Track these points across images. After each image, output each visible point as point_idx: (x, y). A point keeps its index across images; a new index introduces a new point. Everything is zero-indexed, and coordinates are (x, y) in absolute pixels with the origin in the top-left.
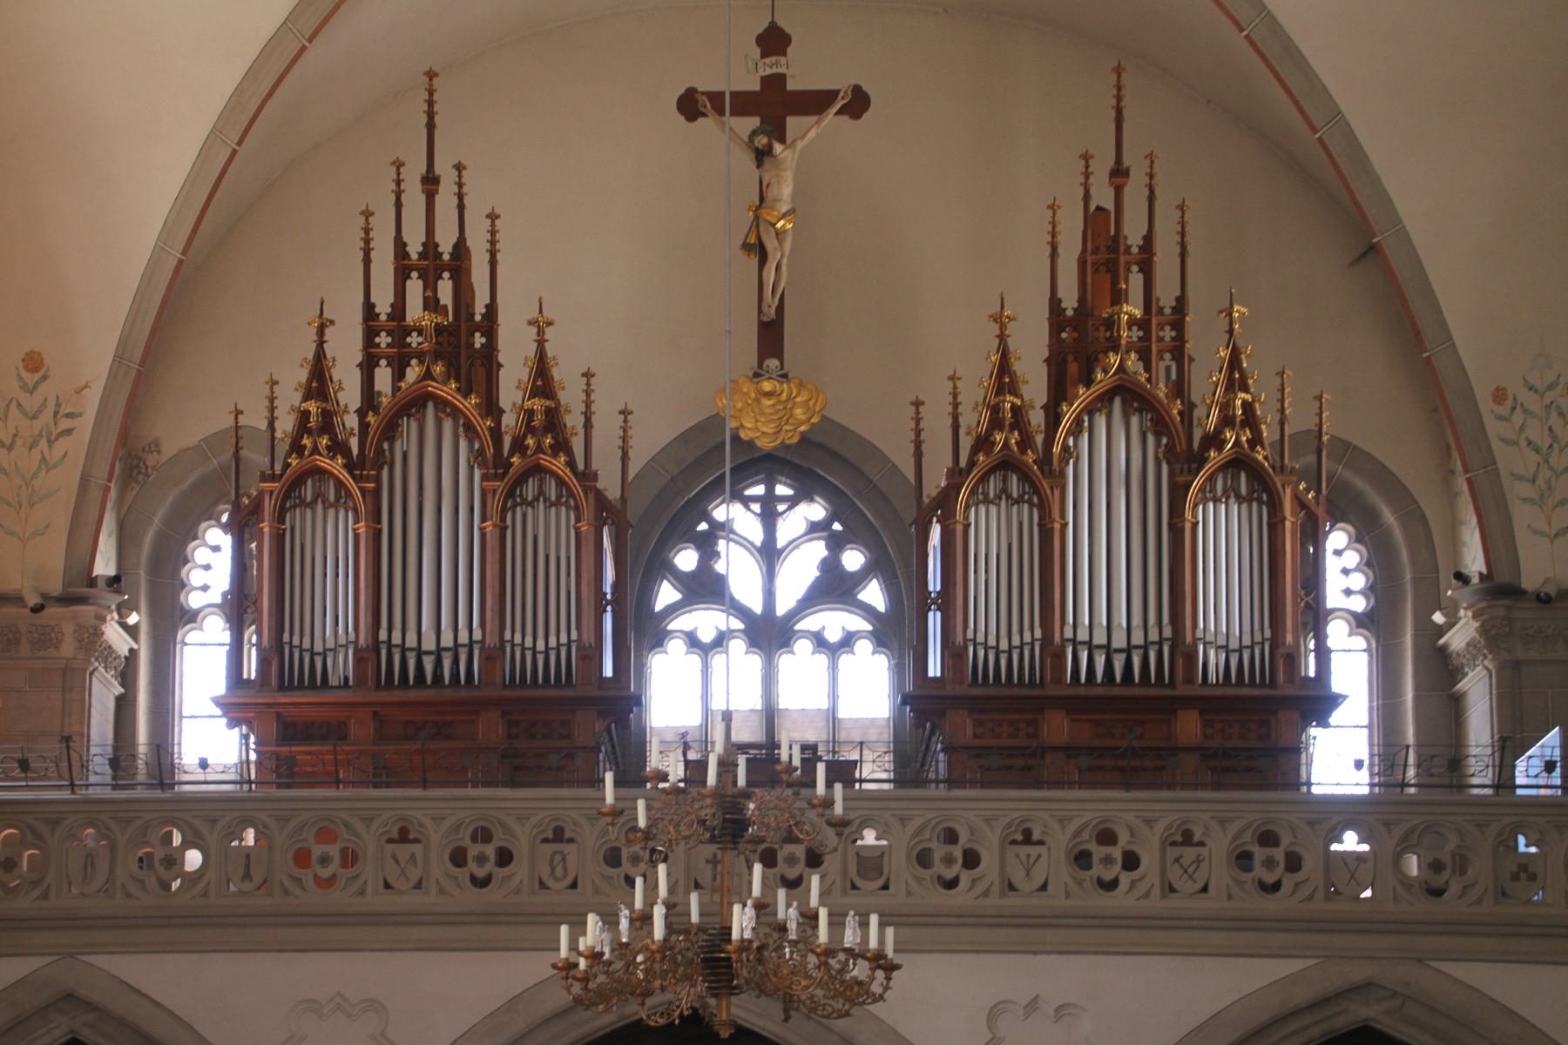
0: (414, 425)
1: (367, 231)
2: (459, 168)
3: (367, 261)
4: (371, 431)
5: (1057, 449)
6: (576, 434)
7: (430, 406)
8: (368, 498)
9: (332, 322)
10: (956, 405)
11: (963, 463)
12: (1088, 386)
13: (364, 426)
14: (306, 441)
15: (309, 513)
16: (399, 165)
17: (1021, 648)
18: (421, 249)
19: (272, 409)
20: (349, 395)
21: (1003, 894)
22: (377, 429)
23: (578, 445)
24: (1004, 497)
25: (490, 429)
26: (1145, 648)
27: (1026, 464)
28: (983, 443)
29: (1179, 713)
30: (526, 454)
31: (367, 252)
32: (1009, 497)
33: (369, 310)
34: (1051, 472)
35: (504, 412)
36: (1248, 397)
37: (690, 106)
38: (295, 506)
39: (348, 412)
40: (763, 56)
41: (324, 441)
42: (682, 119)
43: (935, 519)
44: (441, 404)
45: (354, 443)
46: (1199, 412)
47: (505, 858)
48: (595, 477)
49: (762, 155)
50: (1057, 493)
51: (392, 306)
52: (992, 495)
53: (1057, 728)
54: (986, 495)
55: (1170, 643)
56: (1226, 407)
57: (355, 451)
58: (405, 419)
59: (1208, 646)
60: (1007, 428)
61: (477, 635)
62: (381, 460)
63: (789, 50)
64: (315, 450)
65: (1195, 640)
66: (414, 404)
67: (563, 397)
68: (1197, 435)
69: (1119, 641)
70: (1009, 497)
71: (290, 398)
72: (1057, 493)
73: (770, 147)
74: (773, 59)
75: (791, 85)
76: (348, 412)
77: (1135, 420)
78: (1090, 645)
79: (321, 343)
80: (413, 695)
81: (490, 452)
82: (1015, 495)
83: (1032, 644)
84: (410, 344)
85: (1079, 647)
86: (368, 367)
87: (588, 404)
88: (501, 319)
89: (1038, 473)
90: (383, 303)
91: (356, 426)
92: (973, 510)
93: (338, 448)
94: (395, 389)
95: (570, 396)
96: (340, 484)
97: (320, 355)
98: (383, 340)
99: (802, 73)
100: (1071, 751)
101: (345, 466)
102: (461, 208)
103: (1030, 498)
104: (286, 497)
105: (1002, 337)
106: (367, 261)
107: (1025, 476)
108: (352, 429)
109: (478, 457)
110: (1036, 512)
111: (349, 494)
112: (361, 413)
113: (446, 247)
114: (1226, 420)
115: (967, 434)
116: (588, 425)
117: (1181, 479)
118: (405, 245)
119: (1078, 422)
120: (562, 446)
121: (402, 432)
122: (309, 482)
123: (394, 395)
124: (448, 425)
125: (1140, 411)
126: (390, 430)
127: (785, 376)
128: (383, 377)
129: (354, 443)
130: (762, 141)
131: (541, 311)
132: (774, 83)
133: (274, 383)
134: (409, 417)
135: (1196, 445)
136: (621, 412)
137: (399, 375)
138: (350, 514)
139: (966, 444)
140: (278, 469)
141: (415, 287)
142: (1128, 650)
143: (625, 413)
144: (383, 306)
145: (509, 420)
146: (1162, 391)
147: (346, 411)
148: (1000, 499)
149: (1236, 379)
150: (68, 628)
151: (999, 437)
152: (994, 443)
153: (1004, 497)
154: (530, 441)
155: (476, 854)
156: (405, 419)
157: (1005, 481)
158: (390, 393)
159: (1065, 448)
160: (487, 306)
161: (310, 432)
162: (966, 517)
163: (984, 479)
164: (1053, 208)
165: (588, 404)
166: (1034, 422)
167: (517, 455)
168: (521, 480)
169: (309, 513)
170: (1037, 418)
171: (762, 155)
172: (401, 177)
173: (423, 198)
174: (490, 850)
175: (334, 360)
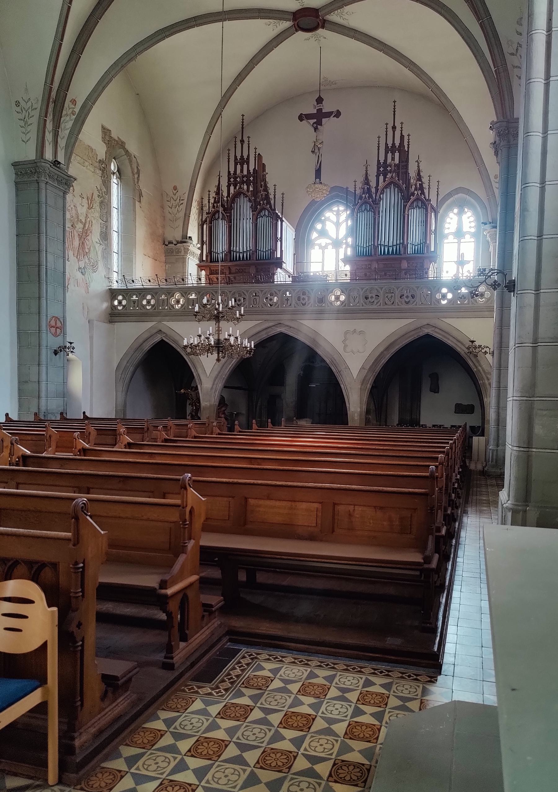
0: (239, 199)
5: (378, 198)
13: (227, 200)
23: (272, 202)
28: (361, 198)
44: (244, 194)
48: (275, 210)
50: (377, 208)
54: (362, 210)
56: (416, 185)
62: (231, 208)
64: (217, 206)
66: (238, 195)
71: (213, 195)
77: (396, 189)
87: (275, 192)
98: (232, 180)
101: (223, 210)
114: (416, 189)
116: (275, 197)
119: (383, 190)
120: (269, 203)
125: (398, 187)
126: (233, 201)
127: (321, 183)
137: (235, 188)
139: (357, 198)
143: (283, 194)
150: (182, 248)
154: (261, 202)
159: (380, 197)
163: (361, 205)
165: (275, 192)
170: (373, 190)
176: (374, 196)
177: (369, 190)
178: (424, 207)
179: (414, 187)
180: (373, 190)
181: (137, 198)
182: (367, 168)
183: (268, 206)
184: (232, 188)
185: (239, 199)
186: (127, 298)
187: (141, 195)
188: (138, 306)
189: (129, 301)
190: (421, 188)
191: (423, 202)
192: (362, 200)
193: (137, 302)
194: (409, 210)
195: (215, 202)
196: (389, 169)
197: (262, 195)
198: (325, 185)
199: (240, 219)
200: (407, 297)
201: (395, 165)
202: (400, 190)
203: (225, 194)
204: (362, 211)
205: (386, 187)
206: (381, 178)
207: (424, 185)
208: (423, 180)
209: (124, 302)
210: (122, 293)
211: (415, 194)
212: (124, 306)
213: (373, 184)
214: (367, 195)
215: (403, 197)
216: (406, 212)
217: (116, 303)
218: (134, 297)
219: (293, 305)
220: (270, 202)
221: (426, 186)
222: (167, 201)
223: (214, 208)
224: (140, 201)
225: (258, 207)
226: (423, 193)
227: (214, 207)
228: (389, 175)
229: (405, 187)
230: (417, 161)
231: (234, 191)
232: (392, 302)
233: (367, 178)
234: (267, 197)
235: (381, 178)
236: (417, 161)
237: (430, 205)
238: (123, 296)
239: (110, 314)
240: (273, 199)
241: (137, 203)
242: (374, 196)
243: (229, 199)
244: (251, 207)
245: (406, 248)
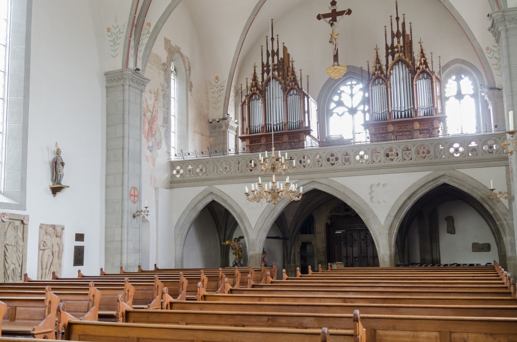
1: (262, 49)
2: (277, 35)
4: (263, 85)
5: (388, 73)
8: (263, 98)
11: (370, 78)
13: (262, 85)
14: (252, 89)
16: (267, 37)
17: (384, 113)
19: (247, 83)
21: (403, 161)
23: (299, 83)
27: (382, 77)
28: (374, 74)
29: (414, 123)
36: (424, 59)
37: (319, 17)
40: (332, 6)
41: (255, 88)
42: (318, 20)
46: (416, 62)
48: (302, 89)
49: (332, 25)
53: (391, 128)
54: (376, 84)
61: (283, 121)
62: (265, 90)
63: (336, 4)
64: (254, 90)
65: (418, 108)
67: (297, 75)
68: (416, 67)
69: (403, 109)
71: (250, 81)
75: (337, 11)
77: (404, 65)
78: (394, 111)
80: (279, 132)
81: (284, 86)
83: (386, 112)
85: (398, 112)
87: (301, 75)
92: (373, 87)
93: (258, 89)
97: (255, 73)
99: (339, 8)
100: (392, 132)
104: (250, 99)
105: (377, 53)
112: (262, 82)
114: (421, 64)
116: (301, 79)
117: (413, 76)
119: (392, 67)
120: (296, 84)
122: (254, 96)
125: (405, 64)
129: (261, 88)
132: (334, 11)
133: (247, 79)
135: (416, 69)
136: (307, 76)
140: (248, 94)
144: (265, 63)
146: (407, 60)
149: (423, 56)
154: (290, 84)
159: (390, 73)
162: (372, 89)
163: (375, 80)
164: (385, 27)
165: (301, 75)
166: (384, 69)
169: (254, 101)
170: (384, 68)
176: (385, 72)
177: (380, 68)
178: (430, 78)
179: (419, 63)
180: (384, 68)
181: (189, 89)
182: (377, 51)
183: (296, 87)
184: (265, 75)
186: (184, 168)
187: (191, 86)
188: (193, 174)
189: (185, 171)
190: (425, 63)
191: (428, 74)
192: (375, 76)
193: (191, 171)
194: (416, 81)
195: (252, 86)
196: (396, 50)
197: (290, 78)
198: (342, 67)
199: (273, 99)
200: (423, 153)
201: (401, 47)
202: (408, 66)
203: (260, 80)
204: (376, 85)
205: (394, 64)
206: (390, 58)
207: (427, 61)
208: (426, 56)
209: (182, 171)
210: (180, 164)
211: (420, 68)
212: (181, 175)
213: (383, 62)
214: (379, 72)
215: (410, 71)
216: (414, 83)
217: (175, 172)
218: (190, 167)
219: (323, 166)
220: (297, 83)
221: (429, 61)
222: (211, 88)
223: (252, 91)
224: (191, 91)
225: (288, 88)
226: (427, 67)
227: (251, 90)
228: (397, 55)
229: (412, 63)
230: (420, 42)
231: (267, 77)
232: (410, 158)
233: (378, 59)
234: (295, 80)
235: (390, 58)
236: (420, 42)
238: (181, 166)
239: (170, 182)
240: (300, 81)
241: (189, 92)
242: (385, 72)
243: (263, 83)
244: (281, 89)
245: (416, 112)
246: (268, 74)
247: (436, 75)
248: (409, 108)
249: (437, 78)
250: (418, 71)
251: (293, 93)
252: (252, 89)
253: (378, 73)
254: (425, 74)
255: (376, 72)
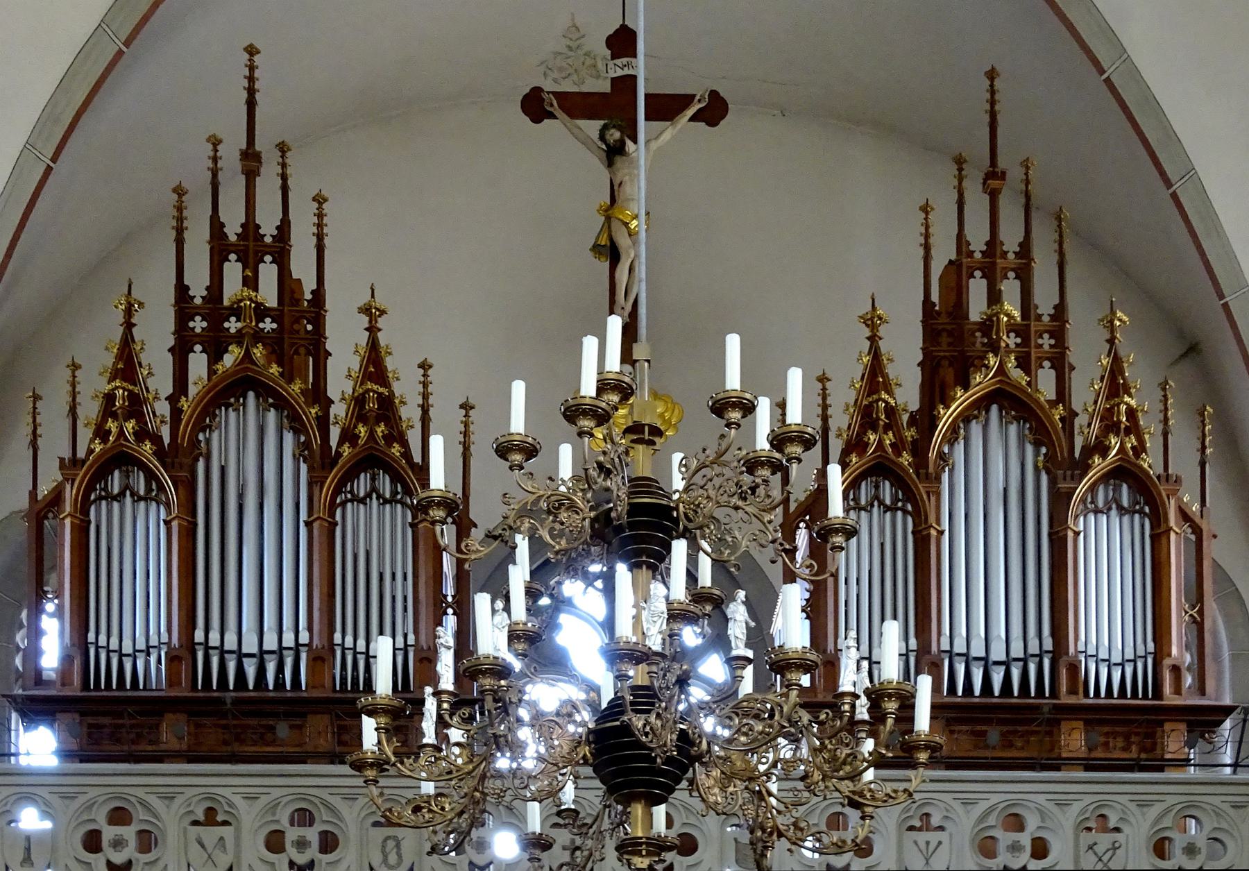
3: (180, 242)
4: (185, 418)
5: (932, 454)
6: (412, 427)
7: (251, 395)
9: (141, 304)
10: (825, 407)
12: (966, 388)
13: (176, 413)
15: (116, 505)
18: (240, 230)
20: (160, 382)
22: (191, 417)
23: (414, 438)
24: (876, 503)
25: (318, 418)
26: (1025, 661)
27: (901, 466)
30: (357, 444)
31: (180, 231)
32: (881, 503)
33: (182, 290)
34: (927, 475)
35: (333, 402)
38: (100, 498)
39: (158, 399)
43: (802, 525)
45: (165, 433)
47: (329, 843)
51: (207, 288)
52: (863, 502)
55: (1050, 655)
57: (167, 440)
58: (223, 408)
59: (1089, 659)
60: (881, 429)
70: (881, 503)
72: (933, 499)
73: (622, 144)
74: (625, 60)
76: (158, 399)
79: (129, 325)
82: (888, 502)
84: (228, 329)
86: (180, 353)
87: (425, 396)
88: (329, 304)
89: (914, 476)
90: (198, 286)
91: (168, 414)
94: (211, 372)
95: (406, 388)
96: (150, 476)
102: (285, 189)
103: (903, 505)
104: (90, 488)
106: (180, 242)
107: (899, 481)
108: (163, 416)
109: (303, 452)
110: (910, 519)
111: (161, 488)
113: (268, 226)
115: (839, 436)
118: (222, 225)
121: (220, 422)
122: (116, 473)
123: (209, 379)
124: (272, 416)
128: (198, 363)
129: (165, 433)
130: (614, 135)
131: (373, 296)
134: (228, 406)
136: (462, 407)
138: (162, 508)
141: (233, 271)
142: (1007, 664)
143: (467, 407)
145: (339, 410)
147: (156, 398)
148: (872, 506)
151: (872, 437)
152: (867, 444)
153: (876, 503)
155: (295, 838)
156: (223, 408)
157: (877, 487)
158: (206, 377)
160: (313, 292)
161: (114, 416)
165: (425, 396)
167: (347, 445)
168: (351, 475)
171: (614, 153)
172: (219, 154)
173: (242, 180)
174: (312, 834)
175: (143, 344)
185: (232, 415)
194: (1077, 517)
237: (1172, 502)
240: (418, 426)
246: (215, 356)
247: (1179, 500)
248: (1013, 655)
249: (1185, 516)
250: (1097, 460)
251: (374, 489)
252: (112, 425)
253: (880, 443)
254: (1125, 487)
255: (872, 437)
